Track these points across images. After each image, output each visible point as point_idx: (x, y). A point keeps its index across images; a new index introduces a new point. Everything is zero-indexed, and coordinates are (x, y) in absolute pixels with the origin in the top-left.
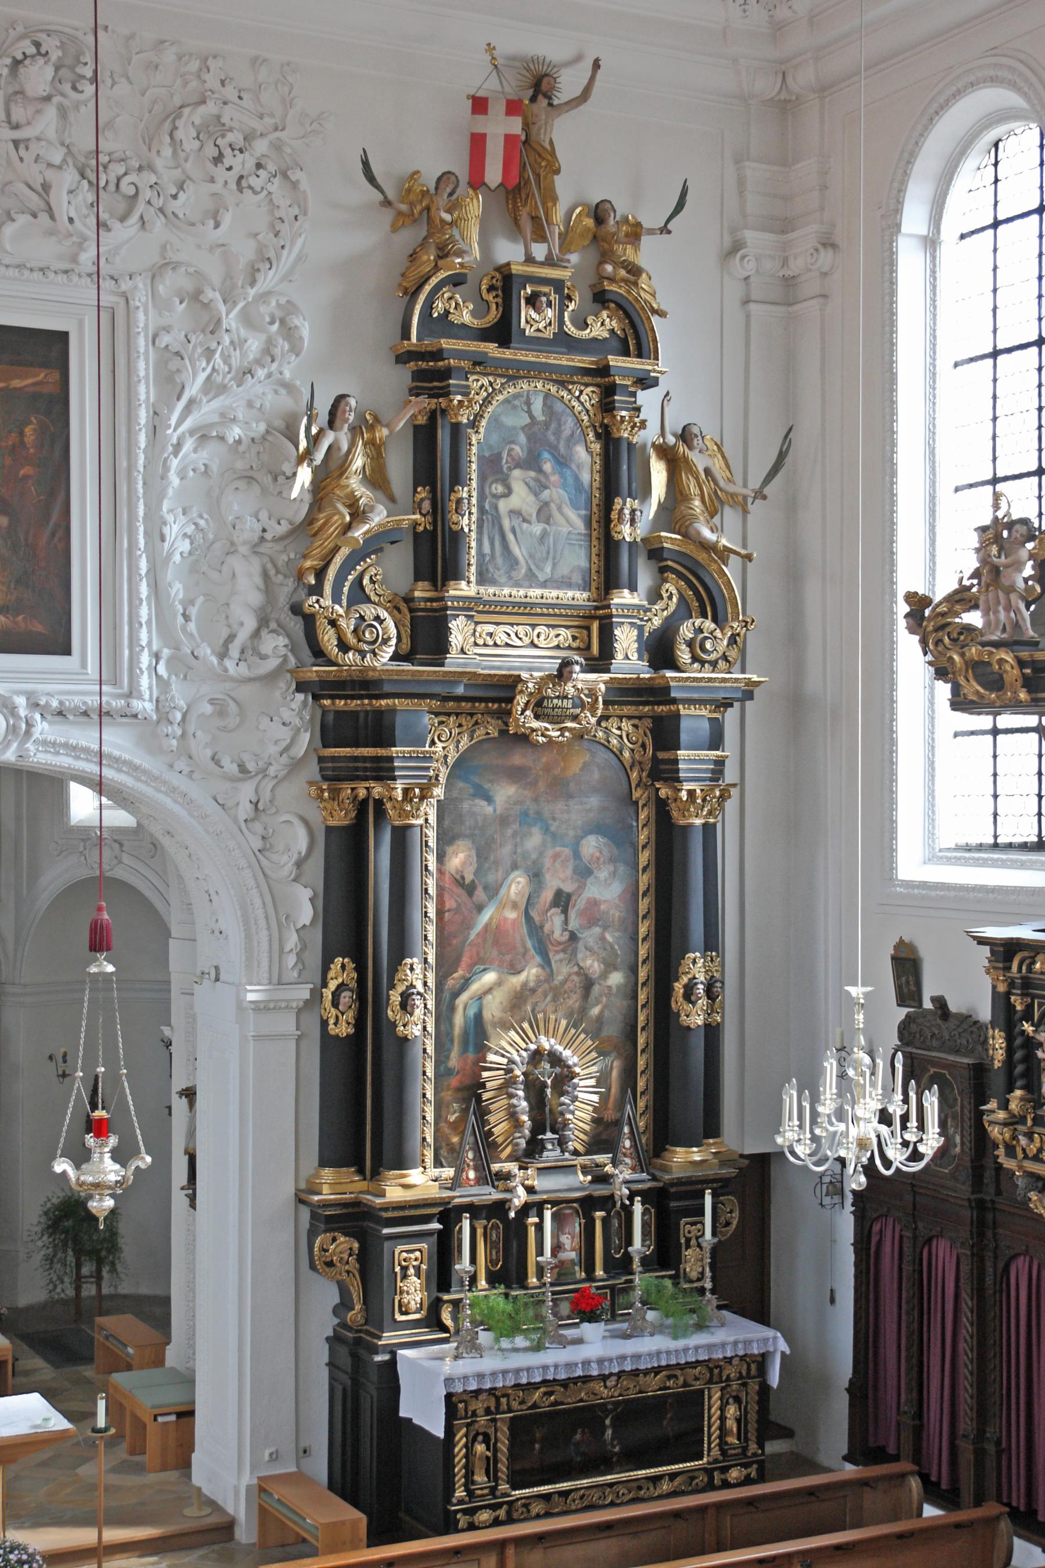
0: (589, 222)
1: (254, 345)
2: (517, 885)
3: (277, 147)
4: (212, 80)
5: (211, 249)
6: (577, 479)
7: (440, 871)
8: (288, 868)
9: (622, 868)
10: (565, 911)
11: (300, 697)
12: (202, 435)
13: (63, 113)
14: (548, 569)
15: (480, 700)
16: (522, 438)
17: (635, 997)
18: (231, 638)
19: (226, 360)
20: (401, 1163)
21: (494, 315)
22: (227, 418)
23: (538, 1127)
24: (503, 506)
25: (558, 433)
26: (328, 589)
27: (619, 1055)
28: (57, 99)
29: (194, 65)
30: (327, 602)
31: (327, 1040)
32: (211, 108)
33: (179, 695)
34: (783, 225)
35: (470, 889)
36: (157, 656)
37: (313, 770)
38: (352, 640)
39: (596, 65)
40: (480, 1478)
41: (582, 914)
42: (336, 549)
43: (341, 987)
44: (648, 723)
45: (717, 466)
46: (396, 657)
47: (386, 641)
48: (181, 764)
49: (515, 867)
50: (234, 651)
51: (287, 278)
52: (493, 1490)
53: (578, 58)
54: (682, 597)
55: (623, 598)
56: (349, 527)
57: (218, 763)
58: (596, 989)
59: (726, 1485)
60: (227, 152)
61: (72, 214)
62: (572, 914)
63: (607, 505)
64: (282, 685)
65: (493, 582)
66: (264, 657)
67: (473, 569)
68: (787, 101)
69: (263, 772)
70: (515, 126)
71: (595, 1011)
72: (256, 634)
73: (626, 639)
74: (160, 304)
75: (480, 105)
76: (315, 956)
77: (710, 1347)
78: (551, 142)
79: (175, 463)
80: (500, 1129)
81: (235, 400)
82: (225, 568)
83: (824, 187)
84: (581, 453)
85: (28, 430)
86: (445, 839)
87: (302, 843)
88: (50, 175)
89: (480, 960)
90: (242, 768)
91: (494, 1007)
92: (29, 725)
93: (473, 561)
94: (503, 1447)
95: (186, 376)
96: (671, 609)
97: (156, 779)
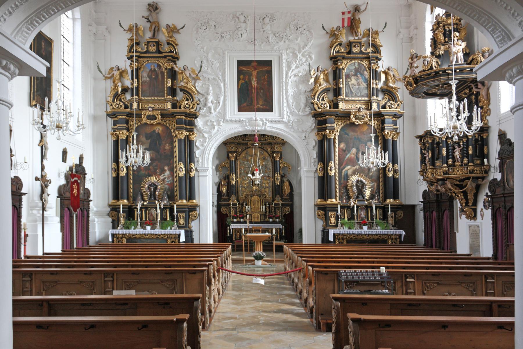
1: (304, 60)
2: (354, 151)
3: (308, 26)
5: (296, 44)
7: (339, 148)
8: (312, 148)
12: (295, 75)
13: (271, 25)
14: (359, 94)
15: (345, 117)
16: (354, 71)
17: (379, 172)
18: (300, 109)
19: (299, 62)
20: (331, 198)
21: (348, 50)
22: (299, 72)
23: (358, 194)
24: (350, 83)
25: (361, 69)
26: (316, 98)
27: (376, 183)
28: (270, 24)
29: (293, 15)
30: (316, 100)
31: (319, 177)
32: (296, 21)
33: (292, 118)
35: (345, 151)
36: (288, 112)
37: (316, 131)
38: (320, 107)
39: (367, 3)
43: (320, 167)
44: (380, 121)
45: (396, 74)
48: (292, 130)
49: (353, 147)
50: (301, 111)
51: (310, 48)
53: (364, 3)
57: (298, 129)
58: (371, 170)
60: (298, 28)
64: (310, 117)
65: (348, 97)
66: (306, 112)
67: (344, 94)
68: (409, 5)
69: (306, 131)
71: (371, 174)
72: (305, 108)
74: (288, 54)
75: (343, 13)
76: (316, 163)
78: (359, 18)
79: (290, 80)
81: (301, 69)
83: (415, 19)
84: (365, 72)
86: (340, 142)
87: (314, 144)
89: (347, 164)
91: (350, 172)
92: (266, 123)
93: (344, 93)
95: (292, 65)
96: (386, 101)
97: (288, 132)
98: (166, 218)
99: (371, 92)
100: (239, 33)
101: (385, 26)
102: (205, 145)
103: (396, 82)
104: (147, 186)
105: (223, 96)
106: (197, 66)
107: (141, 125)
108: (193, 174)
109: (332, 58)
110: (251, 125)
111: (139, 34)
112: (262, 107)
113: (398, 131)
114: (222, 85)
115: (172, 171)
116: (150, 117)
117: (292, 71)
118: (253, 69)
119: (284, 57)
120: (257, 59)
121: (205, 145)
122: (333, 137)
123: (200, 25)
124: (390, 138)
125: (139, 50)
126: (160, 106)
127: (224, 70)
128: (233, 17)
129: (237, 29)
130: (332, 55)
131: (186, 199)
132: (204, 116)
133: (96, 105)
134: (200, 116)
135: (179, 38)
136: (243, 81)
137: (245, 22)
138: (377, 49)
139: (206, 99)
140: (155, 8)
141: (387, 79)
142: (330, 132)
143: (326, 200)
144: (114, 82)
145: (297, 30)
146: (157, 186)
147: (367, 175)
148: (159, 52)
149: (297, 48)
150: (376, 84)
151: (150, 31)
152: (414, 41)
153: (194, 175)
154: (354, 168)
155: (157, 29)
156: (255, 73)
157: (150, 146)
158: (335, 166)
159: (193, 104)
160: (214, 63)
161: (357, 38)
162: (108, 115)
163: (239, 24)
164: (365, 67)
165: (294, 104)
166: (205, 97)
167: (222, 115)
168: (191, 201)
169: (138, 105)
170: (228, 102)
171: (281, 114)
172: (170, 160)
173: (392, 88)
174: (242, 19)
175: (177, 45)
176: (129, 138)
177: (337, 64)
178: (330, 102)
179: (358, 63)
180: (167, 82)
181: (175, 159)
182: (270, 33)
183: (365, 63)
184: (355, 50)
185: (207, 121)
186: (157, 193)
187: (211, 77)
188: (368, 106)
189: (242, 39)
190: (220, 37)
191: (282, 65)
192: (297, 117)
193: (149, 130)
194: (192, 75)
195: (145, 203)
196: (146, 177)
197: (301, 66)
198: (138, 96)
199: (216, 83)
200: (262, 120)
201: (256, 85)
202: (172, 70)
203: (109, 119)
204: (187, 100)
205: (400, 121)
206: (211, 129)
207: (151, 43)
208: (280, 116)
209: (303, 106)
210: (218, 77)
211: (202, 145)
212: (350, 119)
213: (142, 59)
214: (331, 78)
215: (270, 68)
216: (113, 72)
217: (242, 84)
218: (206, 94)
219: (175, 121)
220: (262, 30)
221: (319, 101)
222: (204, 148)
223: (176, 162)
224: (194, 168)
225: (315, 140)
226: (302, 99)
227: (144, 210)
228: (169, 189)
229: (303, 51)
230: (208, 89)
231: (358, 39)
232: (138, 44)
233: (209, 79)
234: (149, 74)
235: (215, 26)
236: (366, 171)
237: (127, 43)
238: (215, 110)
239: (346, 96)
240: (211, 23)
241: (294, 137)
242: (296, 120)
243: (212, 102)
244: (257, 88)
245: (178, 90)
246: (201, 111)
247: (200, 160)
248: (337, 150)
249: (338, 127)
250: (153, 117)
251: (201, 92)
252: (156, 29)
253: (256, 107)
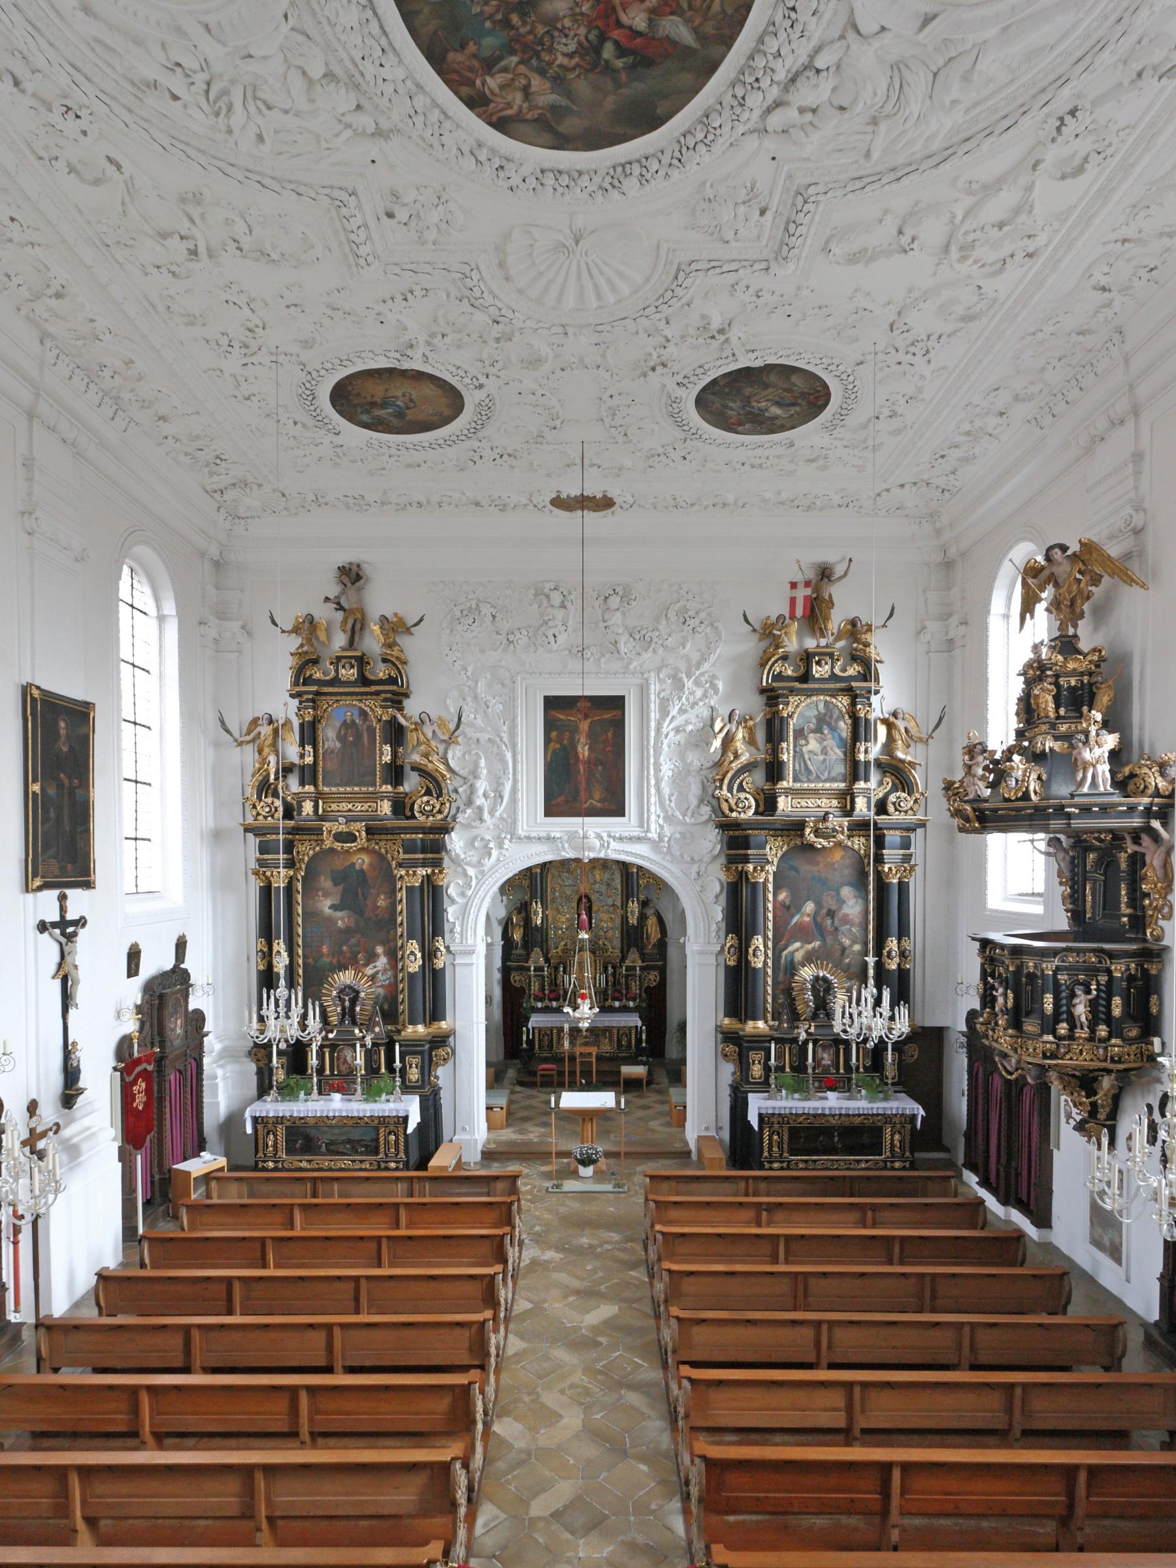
0: (849, 627)
1: (699, 693)
2: (809, 907)
3: (709, 614)
4: (683, 592)
6: (839, 735)
9: (860, 901)
10: (833, 918)
12: (677, 730)
13: (624, 614)
16: (814, 721)
19: (687, 699)
20: (754, 1019)
21: (802, 670)
22: (687, 722)
24: (805, 749)
25: (831, 717)
26: (725, 787)
30: (725, 791)
31: (727, 967)
32: (682, 603)
33: (667, 831)
34: (945, 617)
35: (788, 908)
37: (723, 860)
39: (850, 560)
40: (775, 1149)
41: (840, 920)
42: (727, 772)
43: (732, 946)
45: (911, 726)
46: (756, 813)
47: (749, 807)
48: (668, 858)
49: (808, 899)
51: (713, 665)
52: (781, 1155)
53: (843, 559)
54: (893, 783)
55: (861, 784)
56: (731, 762)
57: (682, 856)
58: (847, 952)
59: (893, 1169)
62: (836, 920)
63: (854, 746)
65: (800, 781)
69: (701, 860)
70: (808, 591)
72: (698, 807)
73: (860, 803)
74: (661, 681)
75: (794, 585)
76: (722, 933)
77: (884, 1109)
78: (830, 596)
79: (666, 742)
80: (800, 1008)
81: (691, 715)
84: (842, 724)
87: (718, 888)
88: (617, 638)
90: (692, 859)
94: (786, 1138)
98: (379, 1068)
99: (855, 771)
100: (550, 633)
101: (891, 615)
102: (469, 893)
103: (912, 744)
104: (335, 993)
105: (510, 782)
106: (452, 710)
107: (322, 851)
108: (439, 964)
109: (763, 691)
110: (573, 848)
111: (317, 638)
112: (599, 805)
113: (912, 863)
114: (509, 756)
115: (394, 956)
116: (340, 837)
117: (671, 721)
119: (652, 687)
120: (586, 693)
121: (469, 893)
122: (762, 880)
123: (458, 614)
124: (895, 881)
125: (318, 675)
126: (366, 806)
127: (514, 720)
128: (536, 595)
129: (546, 623)
130: (764, 684)
131: (424, 1022)
132: (468, 826)
133: (219, 805)
134: (457, 826)
135: (412, 646)
136: (558, 746)
138: (868, 673)
139: (472, 789)
140: (353, 576)
141: (890, 739)
142: (755, 868)
143: (743, 1021)
144: (260, 752)
145: (684, 623)
146: (358, 992)
147: (838, 966)
148: (364, 680)
149: (682, 666)
150: (866, 752)
151: (343, 631)
152: (957, 652)
153: (441, 966)
154: (810, 947)
155: (358, 626)
156: (584, 726)
157: (342, 899)
158: (766, 946)
159: (442, 804)
160: (491, 704)
161: (823, 642)
162: (246, 830)
163: (550, 610)
164: (841, 712)
165: (673, 798)
167: (509, 826)
168: (435, 1025)
169: (316, 807)
170: (522, 796)
171: (642, 822)
172: (388, 932)
173: (902, 761)
174: (556, 598)
175: (405, 663)
176: (294, 882)
177: (777, 704)
178: (758, 794)
179: (826, 702)
180: (382, 754)
181: (399, 930)
182: (620, 631)
183: (843, 702)
184: (818, 671)
185: (474, 839)
186: (358, 1009)
187: (484, 737)
188: (846, 799)
189: (555, 647)
190: (505, 641)
191: (648, 707)
192: (679, 828)
193: (339, 864)
194: (439, 733)
195: (331, 1036)
196: (333, 972)
197: (692, 708)
198: (315, 785)
199: (495, 750)
200: (599, 837)
201: (586, 754)
202: (393, 722)
203: (250, 836)
204: (428, 792)
205: (917, 837)
206: (482, 857)
207: (343, 661)
208: (641, 826)
209: (694, 802)
210: (499, 736)
211: (463, 894)
212: (802, 836)
213: (323, 698)
214: (760, 736)
215: (620, 712)
216: (259, 729)
217: (554, 752)
218: (471, 777)
219: (399, 842)
220: (602, 625)
221: (731, 792)
222: (465, 901)
223: (402, 935)
224: (442, 948)
225: (720, 880)
226: (693, 786)
227: (327, 1051)
228: (385, 998)
229: (698, 673)
230: (476, 764)
231: (827, 646)
232: (315, 662)
234: (340, 731)
235: (494, 617)
236: (837, 955)
237: (290, 661)
238: (492, 812)
239: (796, 780)
240: (486, 610)
241: (670, 872)
242: (678, 836)
243: (485, 795)
244: (589, 762)
245: (407, 768)
246: (459, 815)
247: (458, 929)
248: (770, 906)
249: (773, 852)
250: (350, 837)
251: (461, 772)
252: (356, 626)
253: (586, 806)
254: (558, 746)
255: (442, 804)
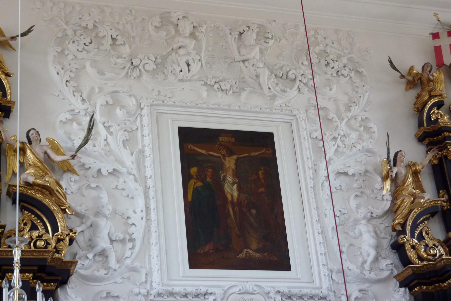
1: (354, 135)
5: (329, 100)
11: (403, 289)
13: (261, 51)
18: (364, 262)
26: (408, 232)
38: (425, 255)
61: (270, 86)
72: (376, 259)
75: (435, 36)
82: (357, 231)
85: (260, 173)
112: (257, 255)
118: (224, 152)
119: (303, 124)
136: (199, 184)
137: (192, 35)
166: (89, 223)
190: (128, 65)
201: (236, 194)
215: (270, 151)
217: (195, 190)
233: (99, 171)
244: (239, 204)
254: (199, 184)
255: (59, 240)
